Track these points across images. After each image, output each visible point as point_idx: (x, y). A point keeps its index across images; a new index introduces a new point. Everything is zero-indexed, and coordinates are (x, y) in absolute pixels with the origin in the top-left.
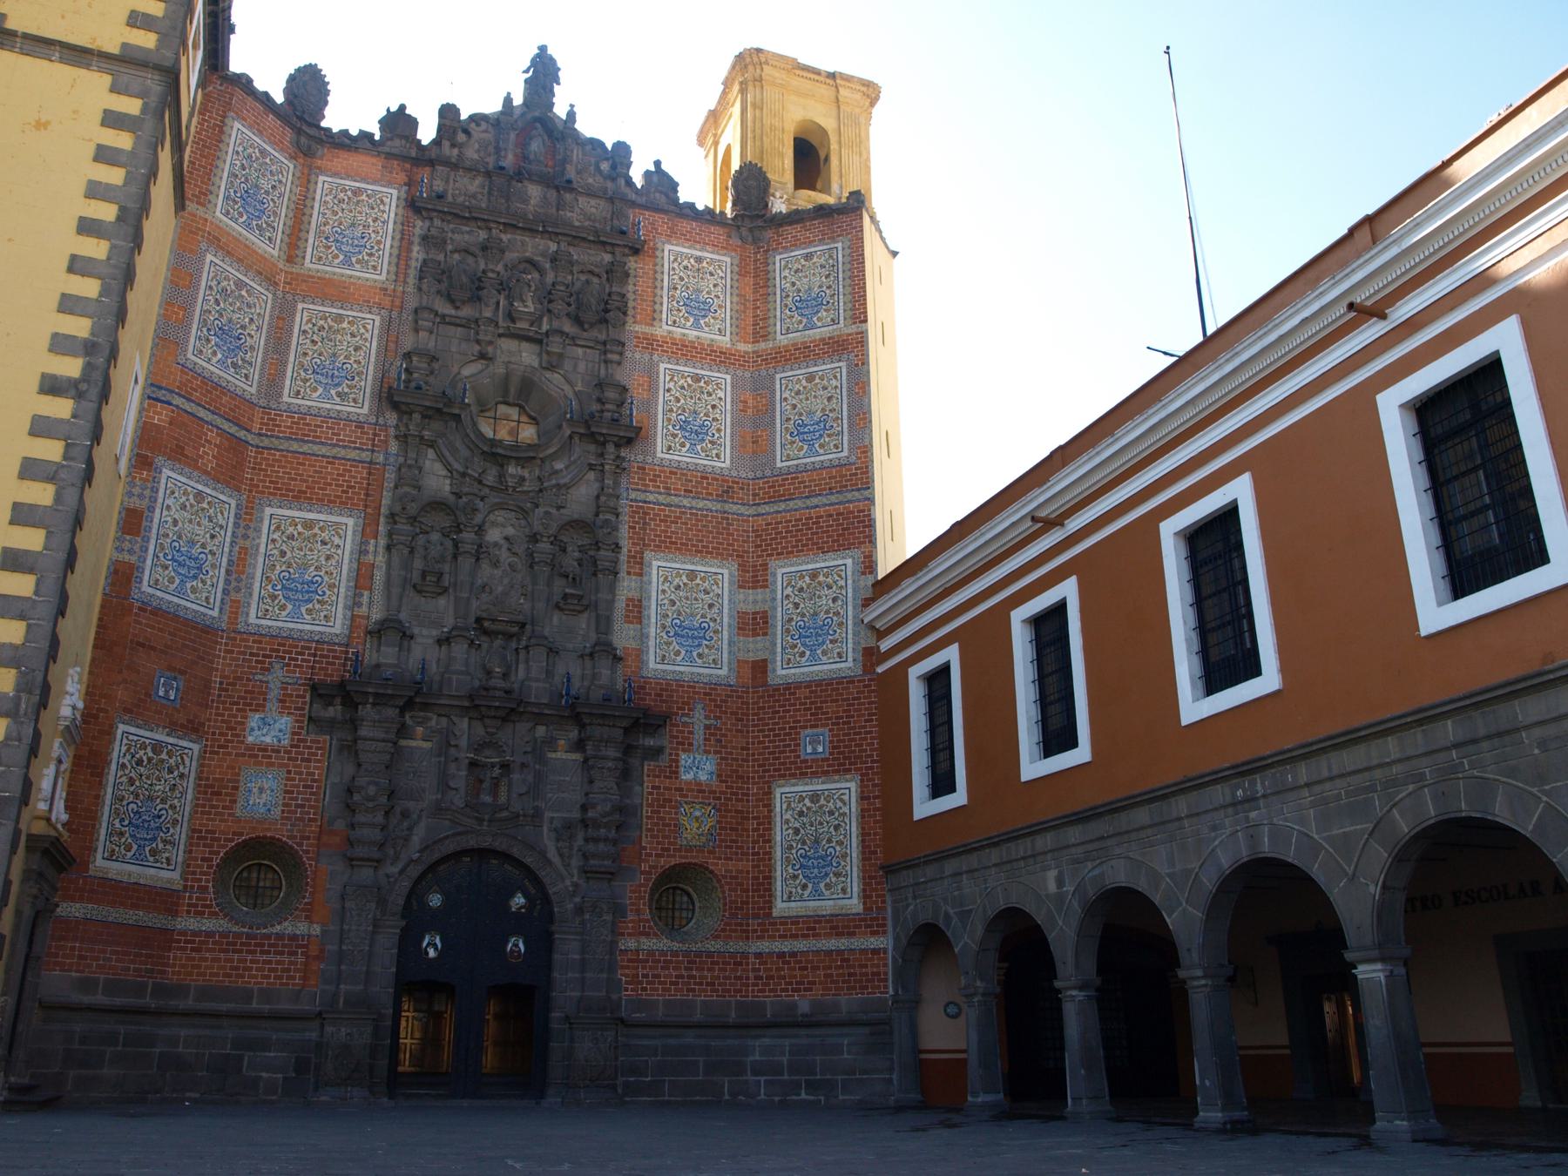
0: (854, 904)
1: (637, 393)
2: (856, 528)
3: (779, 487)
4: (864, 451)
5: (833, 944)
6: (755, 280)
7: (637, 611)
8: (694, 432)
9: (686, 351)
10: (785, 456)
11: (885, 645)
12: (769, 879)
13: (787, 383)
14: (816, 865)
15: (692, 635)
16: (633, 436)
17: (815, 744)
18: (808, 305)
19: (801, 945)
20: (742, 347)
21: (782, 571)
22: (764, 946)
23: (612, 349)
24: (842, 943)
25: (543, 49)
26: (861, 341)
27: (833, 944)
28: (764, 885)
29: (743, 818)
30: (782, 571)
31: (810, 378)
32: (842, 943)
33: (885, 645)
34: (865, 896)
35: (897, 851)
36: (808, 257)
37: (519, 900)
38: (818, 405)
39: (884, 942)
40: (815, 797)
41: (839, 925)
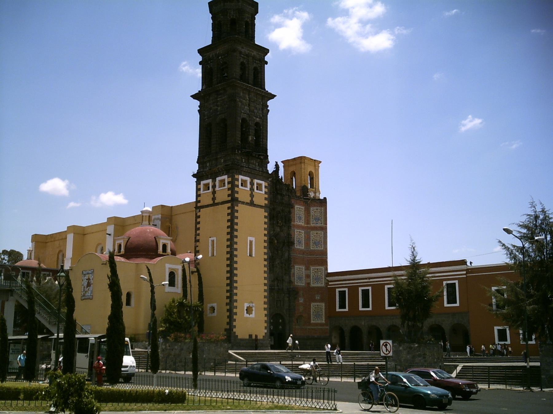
0: (324, 322)
1: (293, 236)
2: (324, 262)
3: (313, 253)
4: (326, 249)
5: (319, 327)
6: (307, 212)
7: (294, 274)
8: (300, 242)
9: (299, 227)
10: (312, 247)
11: (330, 283)
12: (310, 317)
13: (313, 233)
14: (318, 316)
15: (300, 278)
16: (293, 243)
17: (318, 297)
18: (317, 219)
19: (316, 327)
20: (306, 225)
21: (312, 268)
22: (309, 327)
23: (289, 227)
24: (322, 327)
25: (277, 162)
26: (326, 229)
27: (319, 327)
28: (309, 318)
29: (307, 308)
30: (312, 268)
31: (317, 233)
32: (322, 327)
33: (330, 283)
34: (325, 321)
35: (331, 314)
36: (317, 209)
37: (281, 321)
38: (318, 239)
39: (328, 327)
40: (318, 305)
41: (321, 325)
